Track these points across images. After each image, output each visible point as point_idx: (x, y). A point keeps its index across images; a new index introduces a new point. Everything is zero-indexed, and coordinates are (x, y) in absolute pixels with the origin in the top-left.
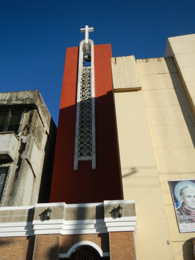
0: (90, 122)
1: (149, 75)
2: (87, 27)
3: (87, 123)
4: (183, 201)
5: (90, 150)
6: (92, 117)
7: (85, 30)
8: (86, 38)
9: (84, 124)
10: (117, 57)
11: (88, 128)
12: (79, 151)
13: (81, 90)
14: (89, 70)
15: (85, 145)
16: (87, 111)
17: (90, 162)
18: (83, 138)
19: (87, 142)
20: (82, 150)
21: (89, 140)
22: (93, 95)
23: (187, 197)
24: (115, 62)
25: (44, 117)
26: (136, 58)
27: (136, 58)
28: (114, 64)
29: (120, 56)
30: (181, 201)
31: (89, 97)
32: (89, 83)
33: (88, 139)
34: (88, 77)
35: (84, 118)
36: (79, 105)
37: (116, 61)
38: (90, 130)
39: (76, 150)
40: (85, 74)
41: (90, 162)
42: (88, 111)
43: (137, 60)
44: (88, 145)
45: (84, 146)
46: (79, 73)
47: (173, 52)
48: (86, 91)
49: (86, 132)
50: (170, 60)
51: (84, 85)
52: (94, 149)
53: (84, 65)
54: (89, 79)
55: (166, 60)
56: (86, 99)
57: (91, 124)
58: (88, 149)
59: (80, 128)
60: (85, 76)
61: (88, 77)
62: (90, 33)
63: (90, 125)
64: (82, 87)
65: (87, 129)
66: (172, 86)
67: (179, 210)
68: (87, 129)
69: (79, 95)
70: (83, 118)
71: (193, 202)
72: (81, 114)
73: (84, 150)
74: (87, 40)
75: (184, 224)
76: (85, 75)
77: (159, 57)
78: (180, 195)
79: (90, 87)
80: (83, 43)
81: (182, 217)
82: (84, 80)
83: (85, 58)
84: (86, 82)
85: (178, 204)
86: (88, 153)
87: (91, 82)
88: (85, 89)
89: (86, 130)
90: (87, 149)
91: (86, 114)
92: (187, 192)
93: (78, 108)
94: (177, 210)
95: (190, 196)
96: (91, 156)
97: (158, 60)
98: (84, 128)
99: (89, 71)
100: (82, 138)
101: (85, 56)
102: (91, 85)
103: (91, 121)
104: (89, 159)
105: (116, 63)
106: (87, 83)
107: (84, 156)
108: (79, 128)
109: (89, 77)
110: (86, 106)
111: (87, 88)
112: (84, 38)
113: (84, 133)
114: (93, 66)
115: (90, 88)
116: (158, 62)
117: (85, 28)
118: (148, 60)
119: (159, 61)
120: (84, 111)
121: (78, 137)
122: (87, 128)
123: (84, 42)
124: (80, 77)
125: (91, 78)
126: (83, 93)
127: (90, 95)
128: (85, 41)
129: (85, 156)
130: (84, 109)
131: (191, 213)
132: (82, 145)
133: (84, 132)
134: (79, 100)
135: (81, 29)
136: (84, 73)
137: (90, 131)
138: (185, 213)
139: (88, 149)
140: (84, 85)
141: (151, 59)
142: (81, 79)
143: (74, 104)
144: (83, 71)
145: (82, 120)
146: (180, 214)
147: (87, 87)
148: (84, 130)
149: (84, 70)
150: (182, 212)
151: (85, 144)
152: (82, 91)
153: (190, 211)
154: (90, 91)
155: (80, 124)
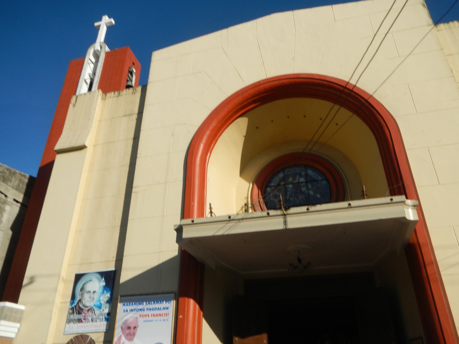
25: (7, 184)
30: (78, 298)
43: (109, 95)
62: (110, 28)
75: (72, 324)
78: (81, 290)
81: (72, 316)
95: (90, 292)
117: (100, 20)
119: (133, 94)
153: (82, 309)
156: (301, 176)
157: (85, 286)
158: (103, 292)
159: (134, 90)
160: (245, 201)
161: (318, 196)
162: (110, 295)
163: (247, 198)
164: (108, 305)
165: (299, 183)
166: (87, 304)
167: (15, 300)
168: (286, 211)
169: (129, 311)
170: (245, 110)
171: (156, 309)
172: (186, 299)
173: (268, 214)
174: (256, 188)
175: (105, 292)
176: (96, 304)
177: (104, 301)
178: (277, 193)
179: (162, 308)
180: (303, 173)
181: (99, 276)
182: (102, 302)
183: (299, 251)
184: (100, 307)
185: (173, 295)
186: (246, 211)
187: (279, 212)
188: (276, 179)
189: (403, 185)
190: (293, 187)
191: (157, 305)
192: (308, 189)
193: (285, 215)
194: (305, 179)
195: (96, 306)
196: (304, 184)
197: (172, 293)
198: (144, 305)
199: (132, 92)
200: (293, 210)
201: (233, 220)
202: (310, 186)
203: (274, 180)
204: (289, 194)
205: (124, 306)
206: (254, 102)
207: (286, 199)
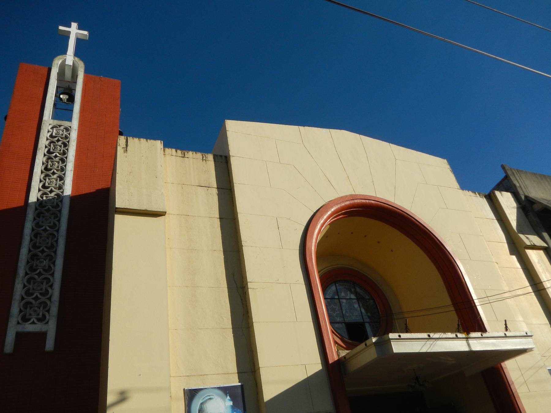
0: (53, 247)
1: (183, 185)
2: (74, 25)
5: (47, 309)
6: (59, 237)
7: (69, 32)
9: (39, 251)
10: (130, 136)
12: (21, 311)
13: (42, 172)
14: (67, 129)
15: (36, 298)
16: (50, 223)
17: (43, 335)
18: (34, 283)
19: (41, 291)
20: (28, 309)
21: (46, 288)
22: (68, 190)
24: (125, 146)
26: (166, 146)
27: (166, 146)
28: (122, 151)
29: (136, 137)
31: (57, 191)
32: (63, 161)
33: (44, 286)
34: (62, 145)
35: (41, 238)
37: (127, 145)
38: (52, 266)
39: (15, 309)
40: (55, 137)
41: (43, 335)
42: (52, 224)
43: (167, 149)
44: (43, 299)
45: (33, 302)
48: (52, 177)
49: (41, 270)
50: (221, 162)
52: (54, 310)
53: (55, 116)
54: (63, 150)
55: (215, 161)
56: (50, 195)
57: (55, 252)
58: (41, 308)
59: (29, 260)
60: (55, 143)
61: (61, 146)
62: (79, 41)
63: (53, 254)
64: (45, 165)
65: (45, 263)
66: (216, 213)
68: (45, 263)
69: (36, 184)
70: (38, 238)
72: (35, 228)
73: (32, 309)
74: (70, 58)
76: (56, 139)
77: (205, 153)
79: (63, 170)
80: (60, 62)
82: (52, 150)
83: (61, 99)
84: (56, 156)
86: (40, 316)
87: (66, 158)
90: (39, 308)
91: (45, 230)
93: (30, 214)
96: (45, 323)
97: (203, 158)
98: (38, 261)
99: (65, 133)
100: (32, 282)
101: (61, 96)
103: (55, 245)
104: (41, 329)
105: (127, 151)
106: (57, 159)
107: (30, 324)
108: (26, 260)
109: (65, 145)
110: (48, 210)
111: (55, 171)
112: (64, 51)
114: (75, 123)
115: (63, 173)
117: (70, 26)
118: (186, 153)
120: (43, 222)
121: (23, 280)
122: (45, 262)
124: (43, 142)
125: (67, 150)
126: (45, 180)
127: (60, 188)
128: (66, 59)
129: (33, 323)
130: (43, 217)
132: (30, 299)
133: (39, 268)
134: (34, 197)
135: (61, 28)
136: (54, 134)
137: (51, 268)
139: (41, 308)
140: (52, 162)
141: (191, 153)
142: (46, 147)
143: (21, 203)
144: (52, 128)
147: (56, 167)
148: (37, 266)
151: (37, 296)
152: (43, 176)
154: (61, 178)
155: (30, 251)
159: (204, 155)
165: (350, 299)
168: (468, 335)
180: (353, 290)
181: (220, 392)
187: (463, 336)
188: (329, 291)
200: (473, 335)
203: (328, 293)
204: (344, 308)
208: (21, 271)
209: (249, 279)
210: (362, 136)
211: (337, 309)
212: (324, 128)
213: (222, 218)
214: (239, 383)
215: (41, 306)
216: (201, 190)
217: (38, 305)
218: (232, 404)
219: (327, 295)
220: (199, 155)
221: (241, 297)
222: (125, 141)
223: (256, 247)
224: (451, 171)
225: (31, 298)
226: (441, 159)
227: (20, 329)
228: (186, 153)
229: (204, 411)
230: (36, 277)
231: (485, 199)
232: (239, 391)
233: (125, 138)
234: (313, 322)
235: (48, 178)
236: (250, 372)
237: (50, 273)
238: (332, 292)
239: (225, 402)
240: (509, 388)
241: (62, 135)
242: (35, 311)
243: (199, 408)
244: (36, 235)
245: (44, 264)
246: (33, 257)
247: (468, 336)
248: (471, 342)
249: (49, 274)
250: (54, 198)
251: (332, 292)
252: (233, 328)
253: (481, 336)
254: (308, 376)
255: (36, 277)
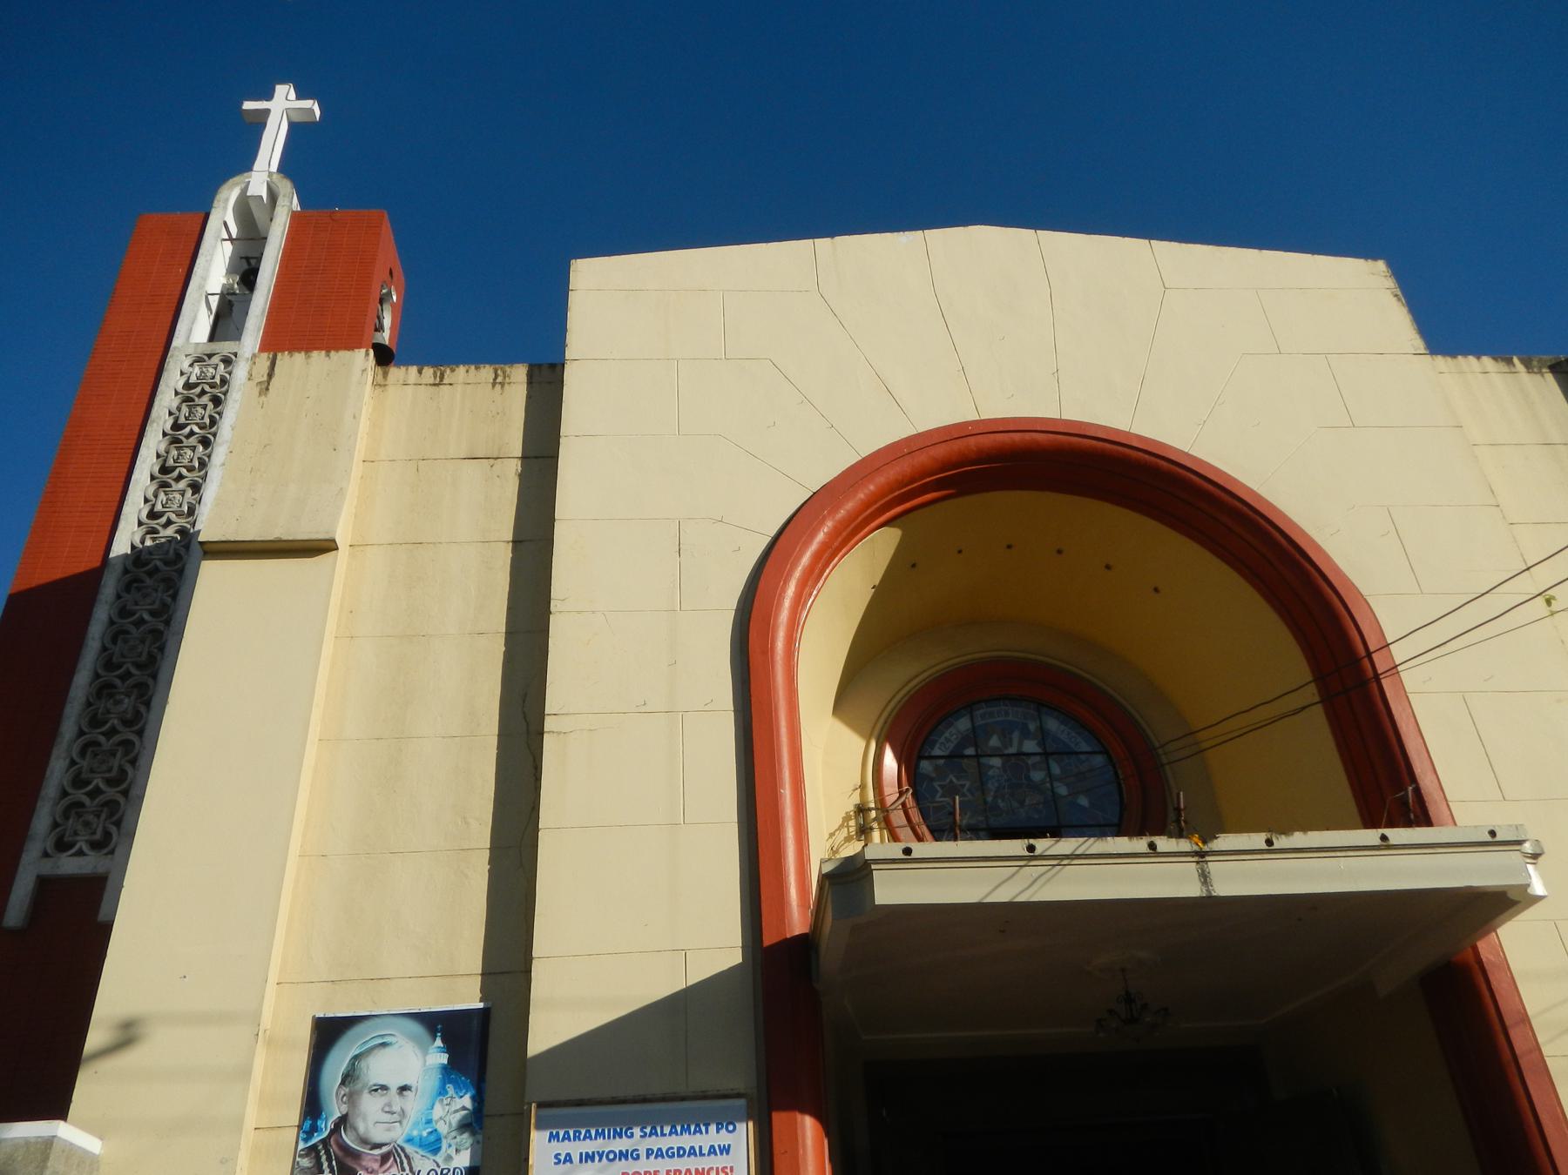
1: (421, 463)
3: (133, 670)
4: (344, 1113)
5: (115, 818)
7: (267, 112)
8: (256, 167)
10: (282, 350)
11: (133, 698)
12: (55, 825)
13: (153, 478)
14: (227, 361)
19: (107, 775)
20: (71, 821)
21: (120, 766)
23: (370, 1092)
24: (265, 378)
29: (299, 350)
30: (334, 1109)
31: (181, 522)
32: (206, 442)
33: (115, 763)
36: (119, 569)
37: (270, 375)
38: (142, 709)
39: (42, 821)
44: (111, 793)
45: (86, 800)
46: (165, 375)
47: (561, 345)
48: (175, 486)
49: (116, 722)
51: (174, 453)
58: (103, 816)
62: (298, 131)
67: (314, 1148)
68: (127, 703)
69: (134, 507)
71: (386, 1112)
72: (116, 619)
73: (81, 820)
76: (198, 390)
77: (505, 364)
78: (343, 1083)
79: (203, 464)
84: (192, 433)
85: (319, 1122)
87: (214, 435)
88: (175, 474)
89: (121, 708)
90: (98, 816)
91: (142, 621)
92: (378, 1069)
93: (109, 586)
94: (302, 1150)
95: (384, 1088)
98: (111, 701)
100: (89, 753)
102: (209, 457)
104: (95, 867)
105: (267, 389)
107: (71, 856)
108: (84, 699)
109: (217, 401)
111: (184, 471)
112: (244, 161)
113: (104, 729)
116: (491, 385)
117: (269, 96)
118: (448, 371)
119: (498, 387)
120: (136, 604)
122: (126, 700)
123: (245, 190)
124: (166, 400)
125: (220, 414)
129: (80, 853)
131: (360, 1165)
132: (80, 795)
135: (248, 105)
136: (193, 379)
138: (334, 1163)
139: (103, 816)
140: (178, 449)
141: (461, 369)
144: (191, 365)
145: (113, 653)
146: (308, 1168)
148: (108, 712)
149: (199, 360)
150: (324, 1158)
153: (356, 1156)
155: (97, 676)
156: (1026, 734)
157: (363, 1064)
158: (442, 1092)
159: (499, 372)
160: (856, 799)
161: (1083, 801)
162: (473, 1099)
163: (863, 787)
164: (466, 1139)
165: (1020, 754)
166: (378, 1135)
167: (58, 1109)
168: (1205, 842)
169: (576, 1158)
170: (908, 505)
171: (681, 1152)
172: (799, 1116)
173: (1152, 846)
174: (890, 761)
175: (450, 1088)
176: (415, 1133)
177: (450, 1123)
178: (954, 780)
179: (705, 1151)
180: (1032, 726)
181: (416, 1028)
182: (443, 1129)
183: (1123, 970)
184: (433, 1145)
185: (742, 1102)
186: (864, 831)
187: (1184, 845)
188: (947, 734)
189: (1418, 792)
190: (1003, 764)
191: (686, 1141)
192: (1050, 775)
193: (1201, 854)
194: (1039, 744)
195: (417, 1140)
196: (1038, 758)
197: (739, 1096)
198: (637, 1140)
199: (492, 381)
200: (1225, 842)
201: (1042, 857)
202: (1056, 770)
203: (942, 739)
204: (992, 786)
205: (554, 1143)
206: (939, 485)
207: (985, 802)
208: (68, 728)
209: (550, 707)
210: (1046, 236)
211: (965, 790)
212: (904, 231)
213: (520, 542)
214: (481, 1001)
215: (102, 811)
216: (473, 469)
217: (95, 809)
218: (446, 1062)
219: (938, 745)
220: (487, 372)
221: (534, 760)
222: (268, 363)
223: (593, 612)
224: (1396, 296)
225: (83, 791)
226: (1362, 261)
227: (47, 868)
228: (448, 371)
229: (358, 1078)
230: (102, 739)
231: (1550, 377)
232: (475, 1025)
233: (271, 356)
234: (739, 822)
235: (164, 491)
236: (522, 972)
237: (136, 728)
238: (955, 736)
239: (425, 1053)
240: (1502, 1038)
241: (213, 378)
242: (87, 824)
243: (348, 1066)
244: (116, 634)
245: (125, 706)
246: (103, 689)
247: (1206, 848)
248: (1215, 867)
249: (133, 732)
250: (171, 540)
251: (955, 736)
252: (492, 849)
253: (1264, 846)
254: (689, 984)
255: (102, 739)
